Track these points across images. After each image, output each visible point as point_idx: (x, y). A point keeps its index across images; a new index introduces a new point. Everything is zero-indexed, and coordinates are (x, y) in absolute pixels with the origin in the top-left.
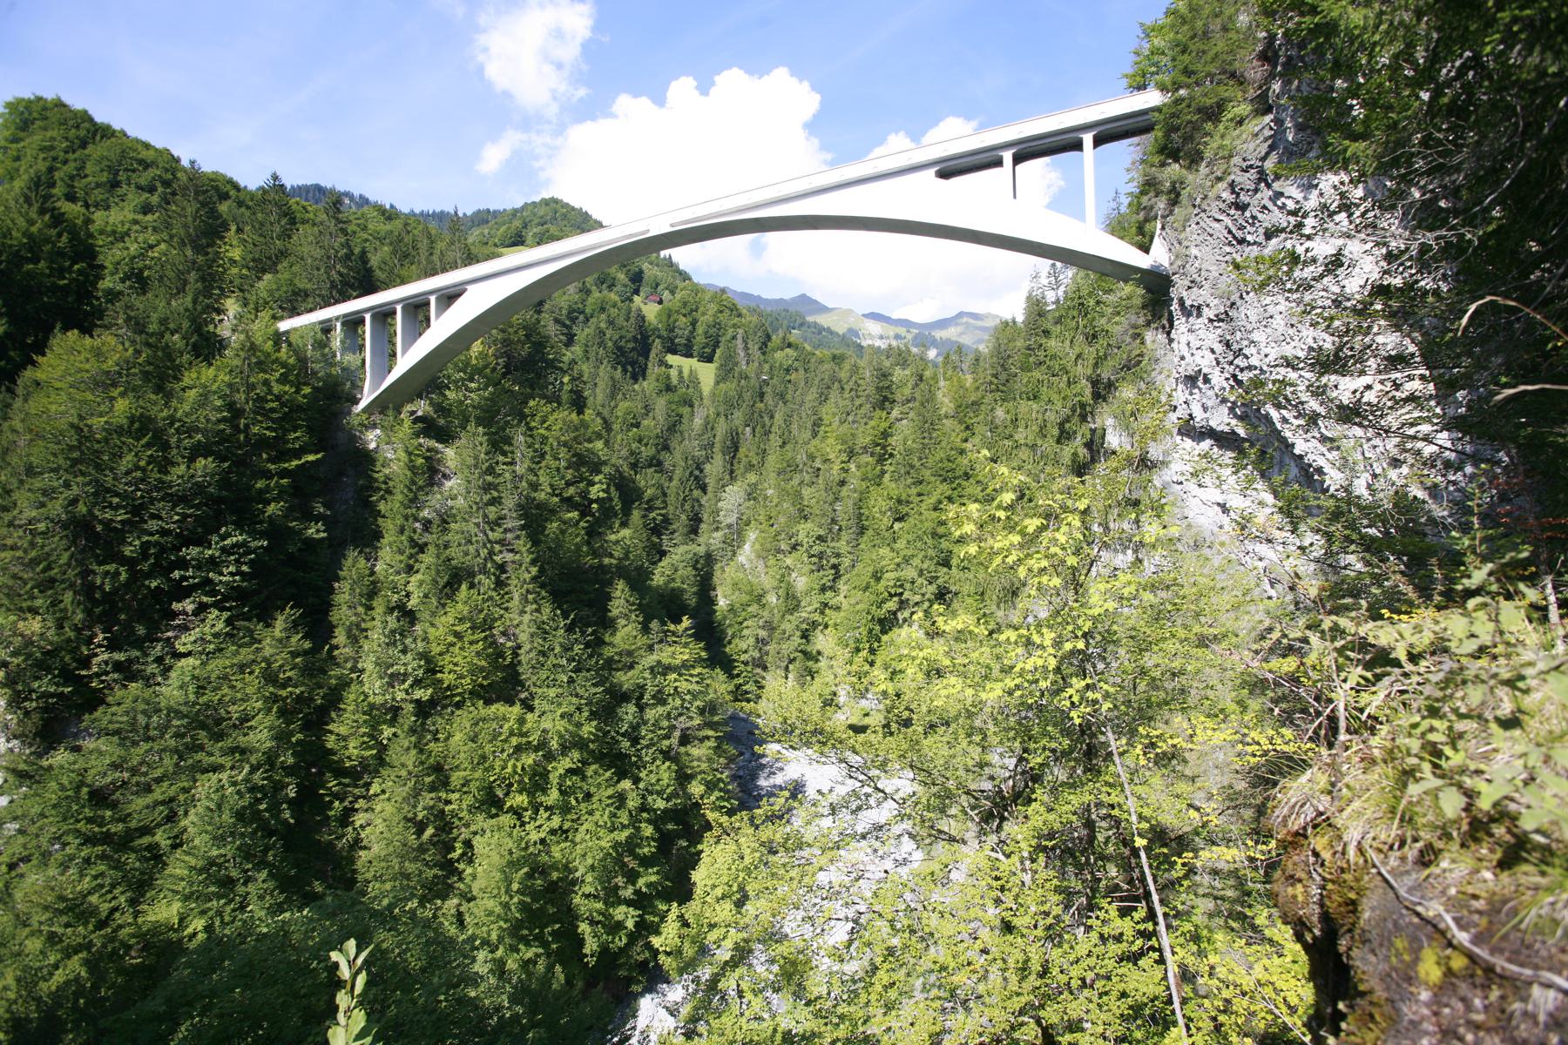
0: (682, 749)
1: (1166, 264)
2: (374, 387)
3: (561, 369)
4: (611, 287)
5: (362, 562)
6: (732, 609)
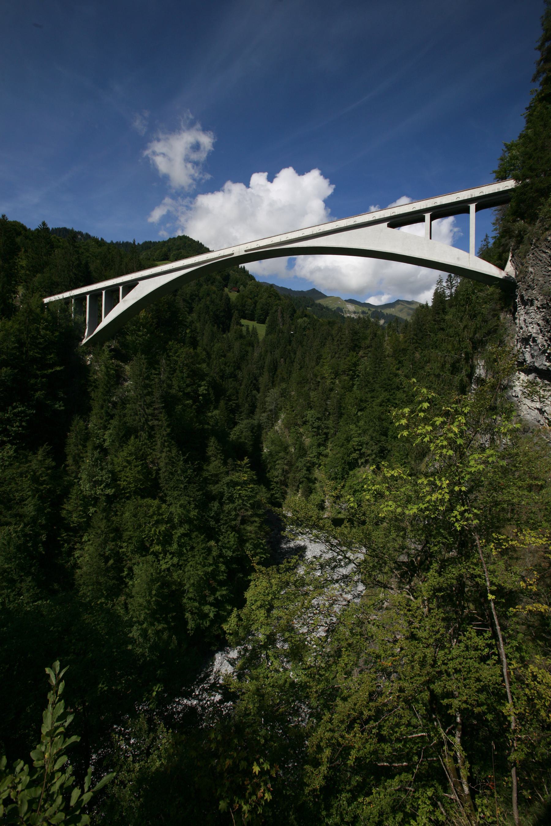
0: (242, 527)
1: (513, 276)
2: (91, 332)
3: (186, 325)
4: (212, 283)
5: (82, 423)
6: (271, 454)
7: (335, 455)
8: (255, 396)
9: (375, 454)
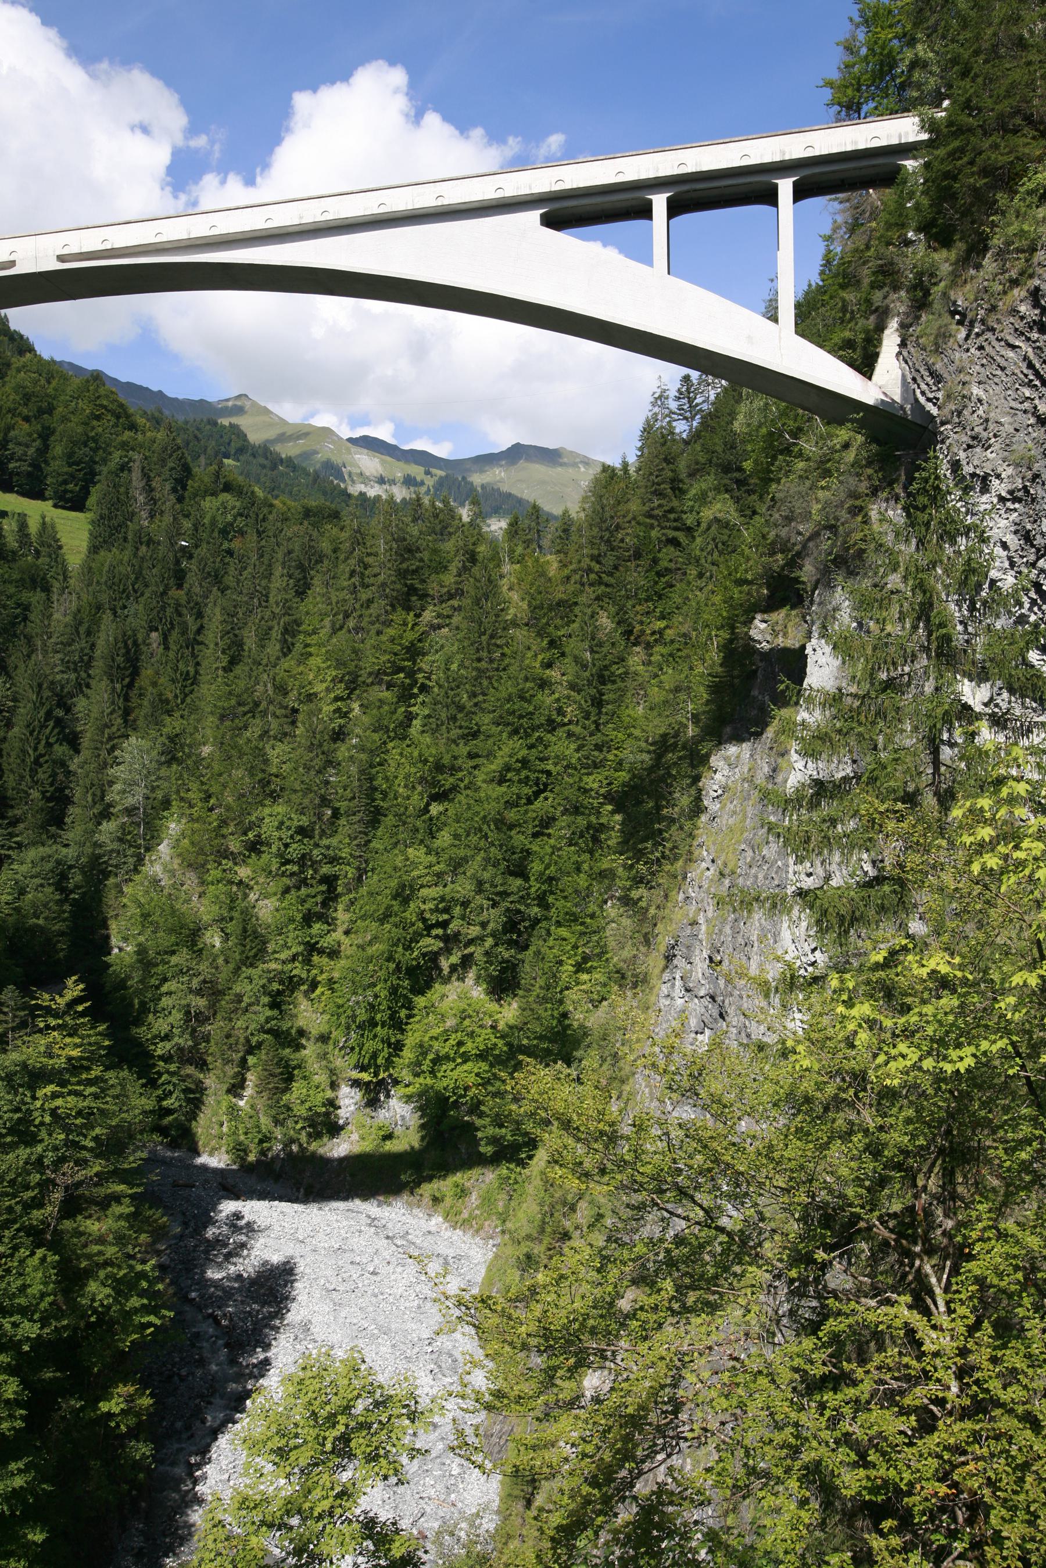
0: (67, 1224)
1: (897, 398)
6: (144, 960)
7: (361, 947)
8: (63, 764)
9: (493, 935)
